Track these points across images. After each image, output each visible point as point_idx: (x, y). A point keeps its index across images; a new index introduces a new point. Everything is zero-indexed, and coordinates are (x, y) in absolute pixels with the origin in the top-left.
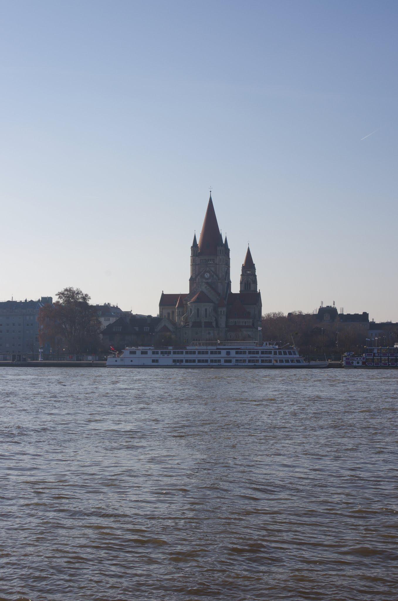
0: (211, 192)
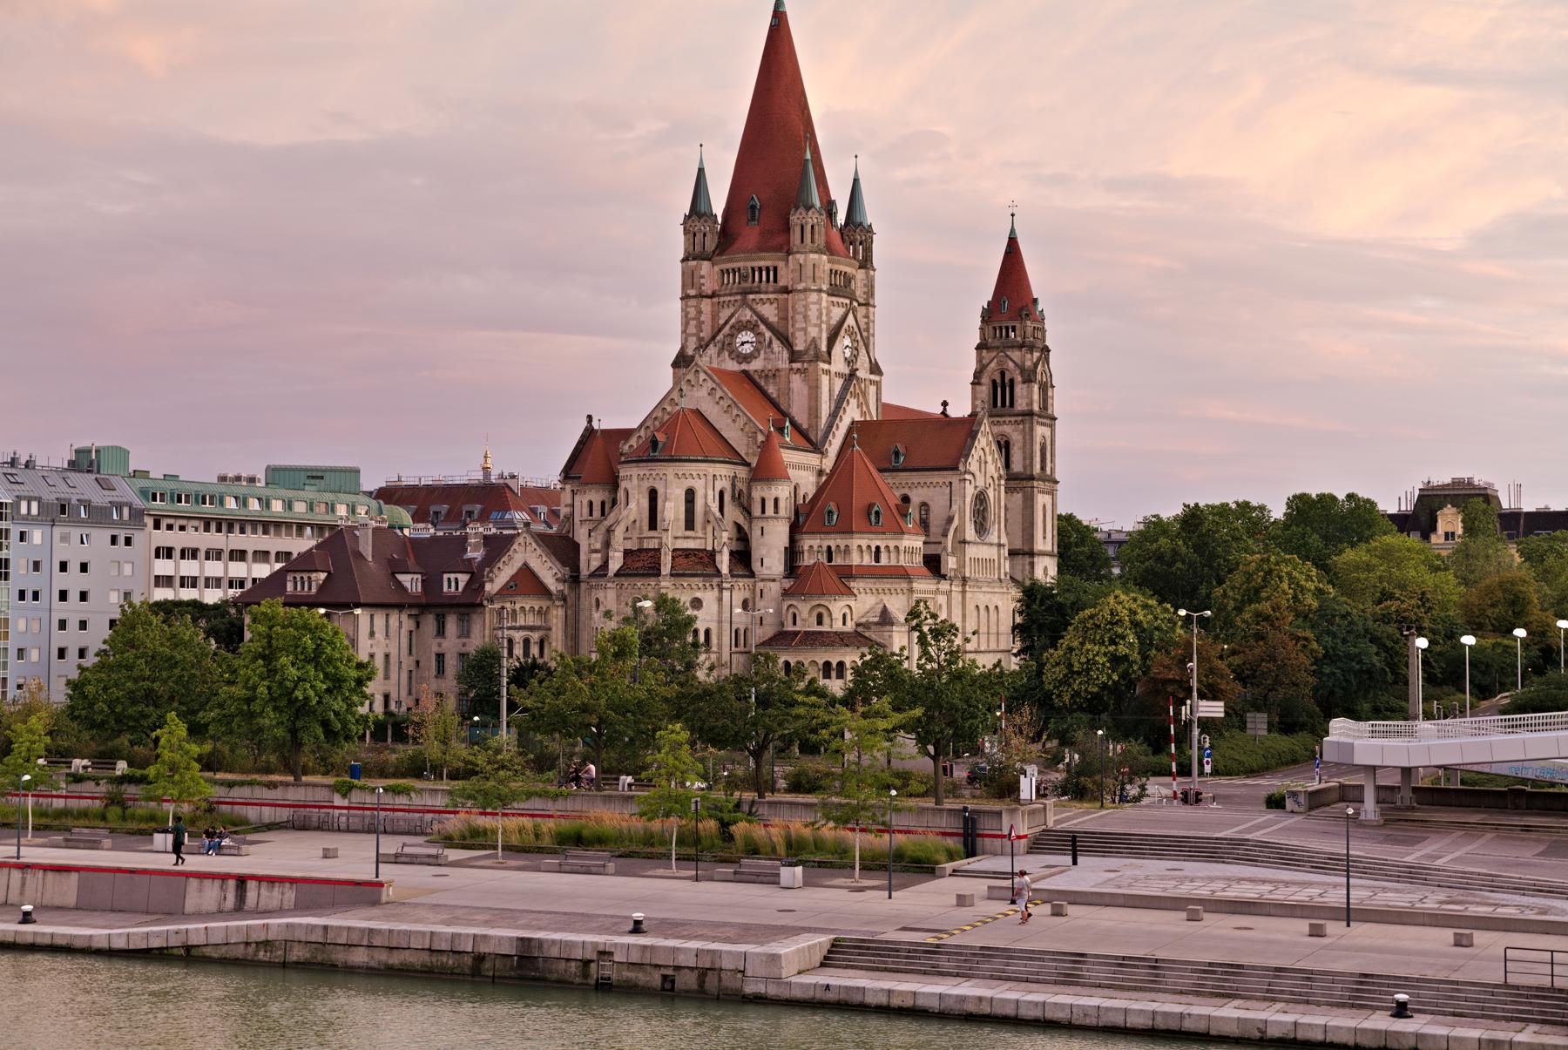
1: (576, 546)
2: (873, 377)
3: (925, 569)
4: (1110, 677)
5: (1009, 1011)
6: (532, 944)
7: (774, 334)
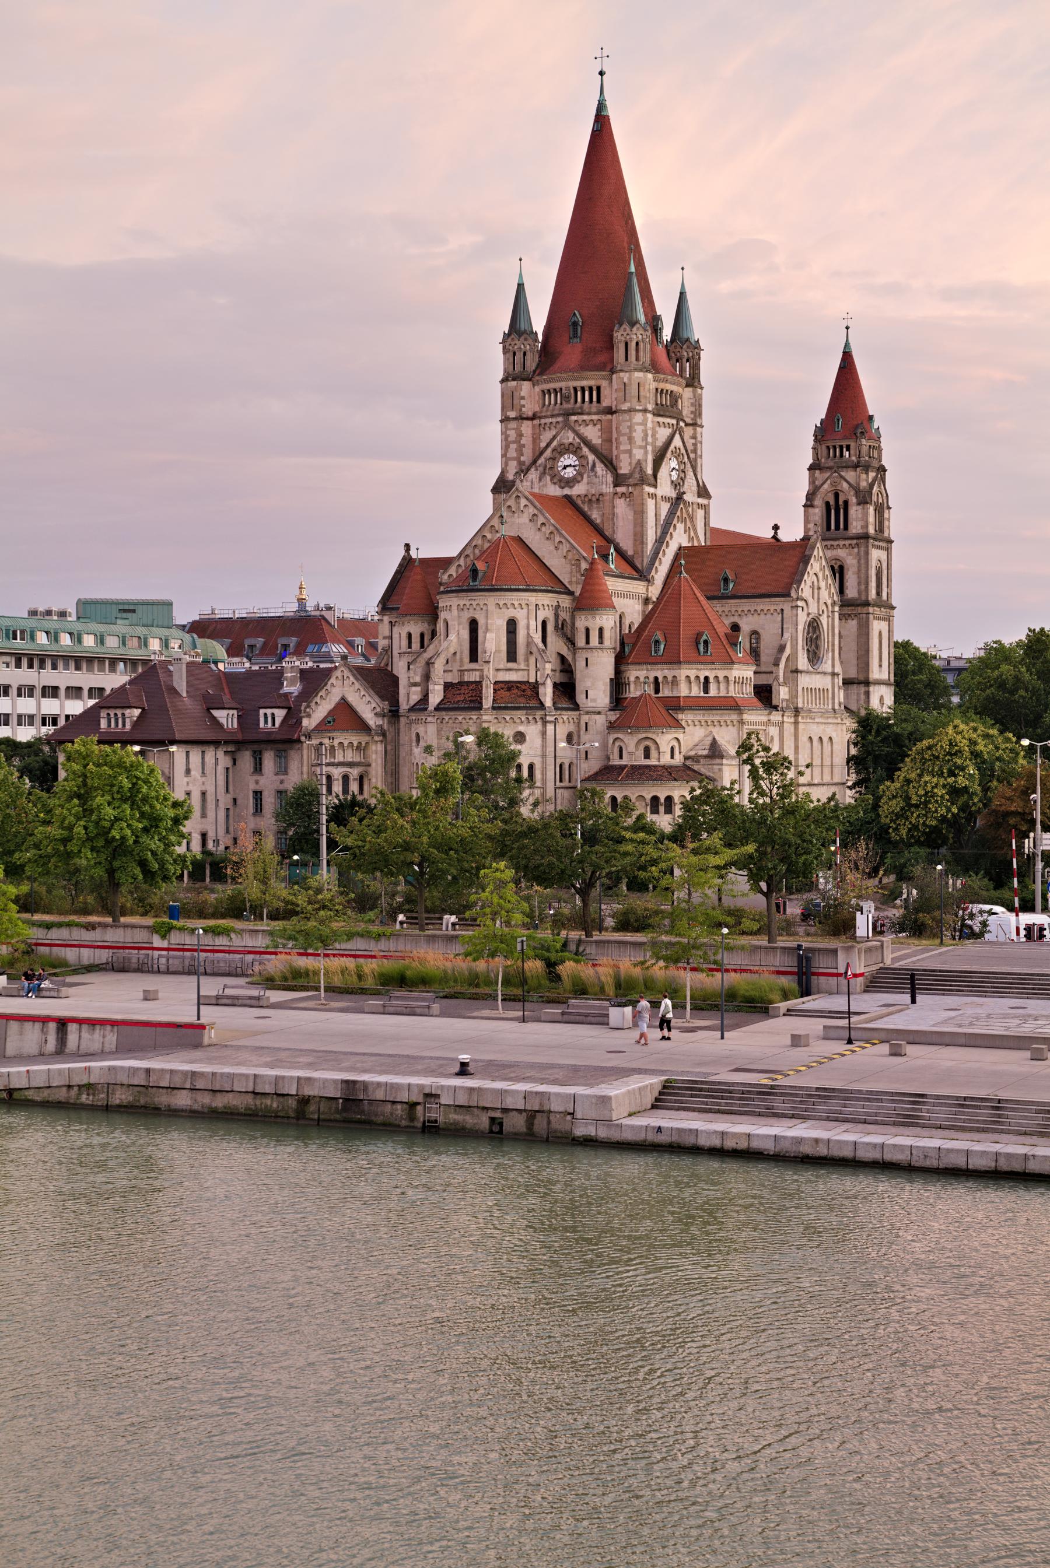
0: (601, 73)
1: (395, 680)
2: (701, 501)
3: (756, 700)
4: (949, 810)
5: (847, 1153)
6: (357, 1086)
7: (598, 457)
